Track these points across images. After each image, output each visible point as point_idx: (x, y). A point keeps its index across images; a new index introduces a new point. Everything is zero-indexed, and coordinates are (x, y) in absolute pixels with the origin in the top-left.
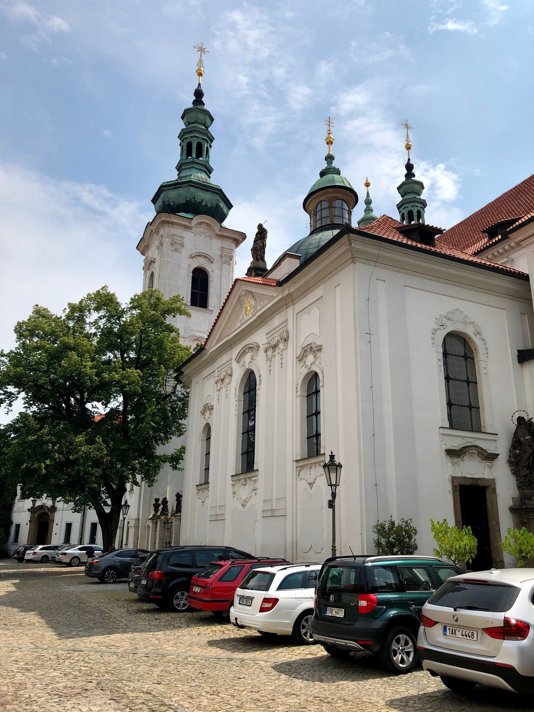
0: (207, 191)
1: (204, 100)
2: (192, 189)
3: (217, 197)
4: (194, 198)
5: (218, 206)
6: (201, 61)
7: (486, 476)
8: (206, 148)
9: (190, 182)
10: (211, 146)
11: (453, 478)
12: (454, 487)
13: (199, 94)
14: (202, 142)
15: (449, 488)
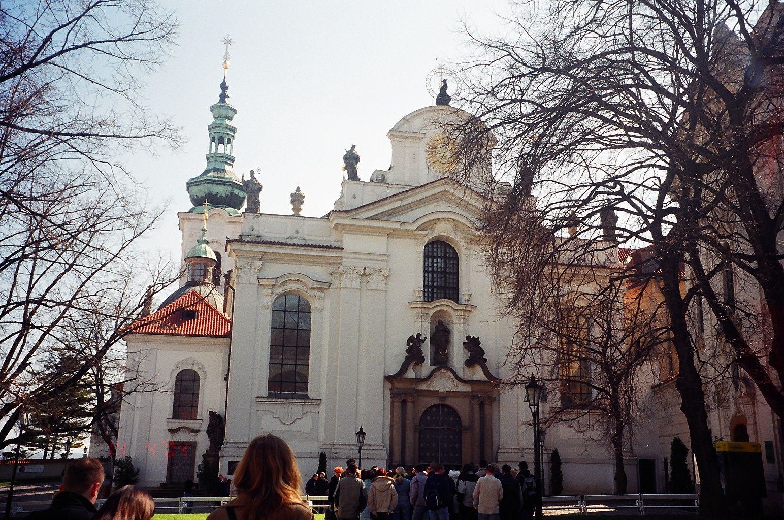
0: (221, 184)
1: (228, 93)
2: (209, 185)
3: (229, 188)
4: (210, 192)
5: (232, 194)
6: (227, 53)
7: (191, 441)
8: (227, 140)
9: (207, 180)
10: (233, 136)
11: (170, 442)
12: (170, 446)
13: (224, 87)
14: (223, 135)
15: (167, 447)
